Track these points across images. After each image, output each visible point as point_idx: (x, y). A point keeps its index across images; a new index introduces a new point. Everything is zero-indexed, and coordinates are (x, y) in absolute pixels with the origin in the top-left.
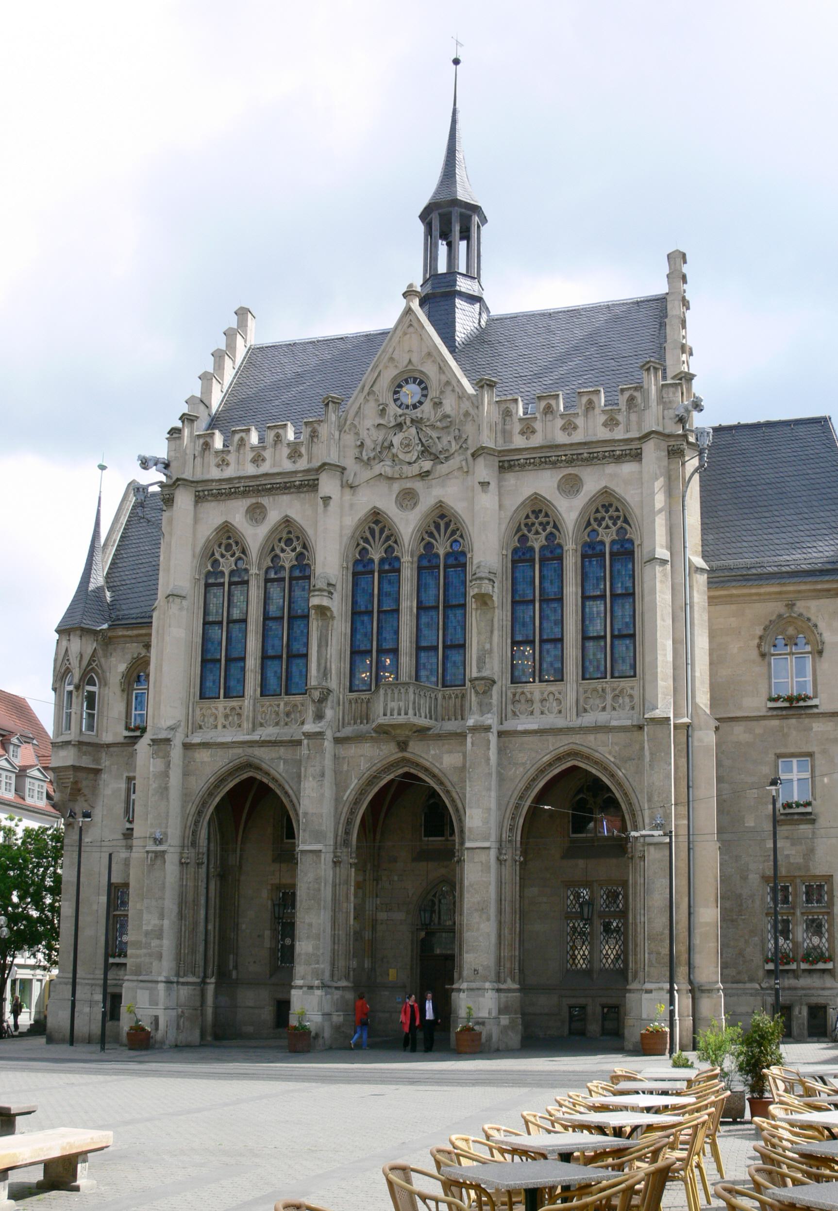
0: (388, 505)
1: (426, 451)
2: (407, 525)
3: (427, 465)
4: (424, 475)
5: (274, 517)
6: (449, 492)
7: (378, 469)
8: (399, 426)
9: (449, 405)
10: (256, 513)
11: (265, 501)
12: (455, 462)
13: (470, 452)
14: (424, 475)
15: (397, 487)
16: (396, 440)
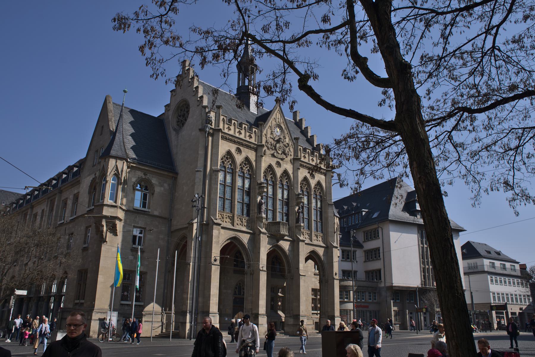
0: (274, 164)
1: (284, 153)
2: (279, 172)
3: (284, 157)
4: (282, 159)
5: (244, 155)
6: (289, 168)
7: (272, 152)
8: (278, 141)
9: (287, 140)
10: (239, 151)
11: (241, 148)
12: (289, 158)
13: (292, 157)
14: (282, 159)
15: (276, 160)
16: (278, 145)
